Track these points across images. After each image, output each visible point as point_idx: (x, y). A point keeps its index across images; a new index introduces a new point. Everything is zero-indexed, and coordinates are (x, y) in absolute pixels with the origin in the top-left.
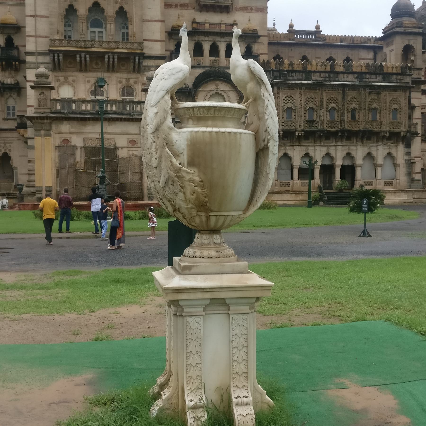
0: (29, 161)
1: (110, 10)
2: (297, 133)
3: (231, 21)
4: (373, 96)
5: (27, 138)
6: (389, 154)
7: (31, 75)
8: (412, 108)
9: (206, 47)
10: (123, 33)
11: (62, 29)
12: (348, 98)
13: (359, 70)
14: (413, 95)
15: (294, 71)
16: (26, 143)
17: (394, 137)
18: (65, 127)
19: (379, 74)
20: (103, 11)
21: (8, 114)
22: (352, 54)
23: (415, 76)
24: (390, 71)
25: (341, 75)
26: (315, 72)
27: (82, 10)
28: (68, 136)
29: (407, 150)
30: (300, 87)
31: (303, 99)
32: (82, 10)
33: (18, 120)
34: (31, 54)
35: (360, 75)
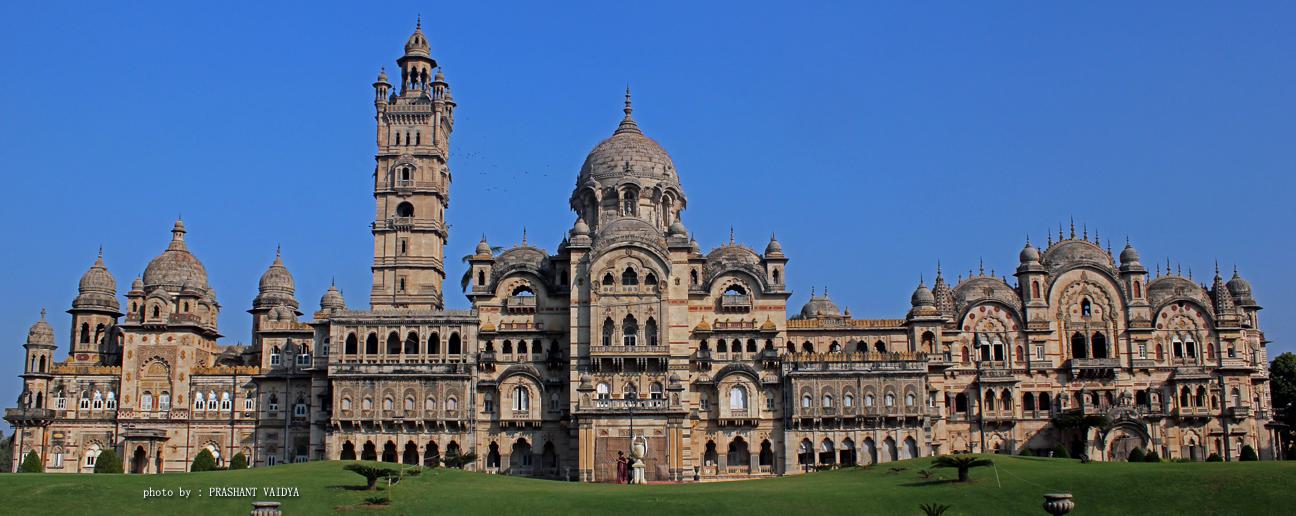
0: (571, 449)
1: (642, 321)
2: (815, 420)
3: (750, 320)
4: (889, 382)
5: (570, 429)
6: (909, 438)
7: (574, 375)
8: (933, 393)
9: (729, 342)
10: (652, 338)
11: (601, 337)
12: (862, 387)
13: (874, 360)
14: (931, 379)
15: (811, 363)
16: (568, 433)
17: (912, 421)
18: (604, 422)
19: (895, 362)
20: (635, 321)
21: (553, 408)
22: (883, 338)
23: (936, 361)
24: (906, 359)
25: (858, 365)
26: (833, 362)
27: (618, 321)
28: (605, 428)
29: (926, 434)
30: (817, 377)
31: (820, 388)
32: (618, 321)
33: (562, 414)
34: (574, 358)
35: (876, 363)
